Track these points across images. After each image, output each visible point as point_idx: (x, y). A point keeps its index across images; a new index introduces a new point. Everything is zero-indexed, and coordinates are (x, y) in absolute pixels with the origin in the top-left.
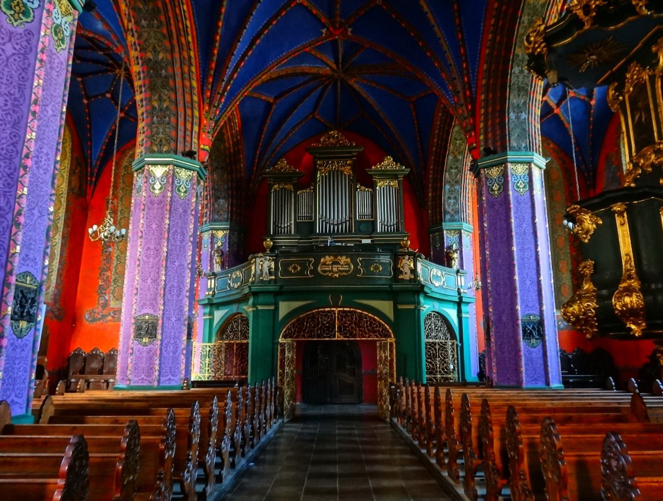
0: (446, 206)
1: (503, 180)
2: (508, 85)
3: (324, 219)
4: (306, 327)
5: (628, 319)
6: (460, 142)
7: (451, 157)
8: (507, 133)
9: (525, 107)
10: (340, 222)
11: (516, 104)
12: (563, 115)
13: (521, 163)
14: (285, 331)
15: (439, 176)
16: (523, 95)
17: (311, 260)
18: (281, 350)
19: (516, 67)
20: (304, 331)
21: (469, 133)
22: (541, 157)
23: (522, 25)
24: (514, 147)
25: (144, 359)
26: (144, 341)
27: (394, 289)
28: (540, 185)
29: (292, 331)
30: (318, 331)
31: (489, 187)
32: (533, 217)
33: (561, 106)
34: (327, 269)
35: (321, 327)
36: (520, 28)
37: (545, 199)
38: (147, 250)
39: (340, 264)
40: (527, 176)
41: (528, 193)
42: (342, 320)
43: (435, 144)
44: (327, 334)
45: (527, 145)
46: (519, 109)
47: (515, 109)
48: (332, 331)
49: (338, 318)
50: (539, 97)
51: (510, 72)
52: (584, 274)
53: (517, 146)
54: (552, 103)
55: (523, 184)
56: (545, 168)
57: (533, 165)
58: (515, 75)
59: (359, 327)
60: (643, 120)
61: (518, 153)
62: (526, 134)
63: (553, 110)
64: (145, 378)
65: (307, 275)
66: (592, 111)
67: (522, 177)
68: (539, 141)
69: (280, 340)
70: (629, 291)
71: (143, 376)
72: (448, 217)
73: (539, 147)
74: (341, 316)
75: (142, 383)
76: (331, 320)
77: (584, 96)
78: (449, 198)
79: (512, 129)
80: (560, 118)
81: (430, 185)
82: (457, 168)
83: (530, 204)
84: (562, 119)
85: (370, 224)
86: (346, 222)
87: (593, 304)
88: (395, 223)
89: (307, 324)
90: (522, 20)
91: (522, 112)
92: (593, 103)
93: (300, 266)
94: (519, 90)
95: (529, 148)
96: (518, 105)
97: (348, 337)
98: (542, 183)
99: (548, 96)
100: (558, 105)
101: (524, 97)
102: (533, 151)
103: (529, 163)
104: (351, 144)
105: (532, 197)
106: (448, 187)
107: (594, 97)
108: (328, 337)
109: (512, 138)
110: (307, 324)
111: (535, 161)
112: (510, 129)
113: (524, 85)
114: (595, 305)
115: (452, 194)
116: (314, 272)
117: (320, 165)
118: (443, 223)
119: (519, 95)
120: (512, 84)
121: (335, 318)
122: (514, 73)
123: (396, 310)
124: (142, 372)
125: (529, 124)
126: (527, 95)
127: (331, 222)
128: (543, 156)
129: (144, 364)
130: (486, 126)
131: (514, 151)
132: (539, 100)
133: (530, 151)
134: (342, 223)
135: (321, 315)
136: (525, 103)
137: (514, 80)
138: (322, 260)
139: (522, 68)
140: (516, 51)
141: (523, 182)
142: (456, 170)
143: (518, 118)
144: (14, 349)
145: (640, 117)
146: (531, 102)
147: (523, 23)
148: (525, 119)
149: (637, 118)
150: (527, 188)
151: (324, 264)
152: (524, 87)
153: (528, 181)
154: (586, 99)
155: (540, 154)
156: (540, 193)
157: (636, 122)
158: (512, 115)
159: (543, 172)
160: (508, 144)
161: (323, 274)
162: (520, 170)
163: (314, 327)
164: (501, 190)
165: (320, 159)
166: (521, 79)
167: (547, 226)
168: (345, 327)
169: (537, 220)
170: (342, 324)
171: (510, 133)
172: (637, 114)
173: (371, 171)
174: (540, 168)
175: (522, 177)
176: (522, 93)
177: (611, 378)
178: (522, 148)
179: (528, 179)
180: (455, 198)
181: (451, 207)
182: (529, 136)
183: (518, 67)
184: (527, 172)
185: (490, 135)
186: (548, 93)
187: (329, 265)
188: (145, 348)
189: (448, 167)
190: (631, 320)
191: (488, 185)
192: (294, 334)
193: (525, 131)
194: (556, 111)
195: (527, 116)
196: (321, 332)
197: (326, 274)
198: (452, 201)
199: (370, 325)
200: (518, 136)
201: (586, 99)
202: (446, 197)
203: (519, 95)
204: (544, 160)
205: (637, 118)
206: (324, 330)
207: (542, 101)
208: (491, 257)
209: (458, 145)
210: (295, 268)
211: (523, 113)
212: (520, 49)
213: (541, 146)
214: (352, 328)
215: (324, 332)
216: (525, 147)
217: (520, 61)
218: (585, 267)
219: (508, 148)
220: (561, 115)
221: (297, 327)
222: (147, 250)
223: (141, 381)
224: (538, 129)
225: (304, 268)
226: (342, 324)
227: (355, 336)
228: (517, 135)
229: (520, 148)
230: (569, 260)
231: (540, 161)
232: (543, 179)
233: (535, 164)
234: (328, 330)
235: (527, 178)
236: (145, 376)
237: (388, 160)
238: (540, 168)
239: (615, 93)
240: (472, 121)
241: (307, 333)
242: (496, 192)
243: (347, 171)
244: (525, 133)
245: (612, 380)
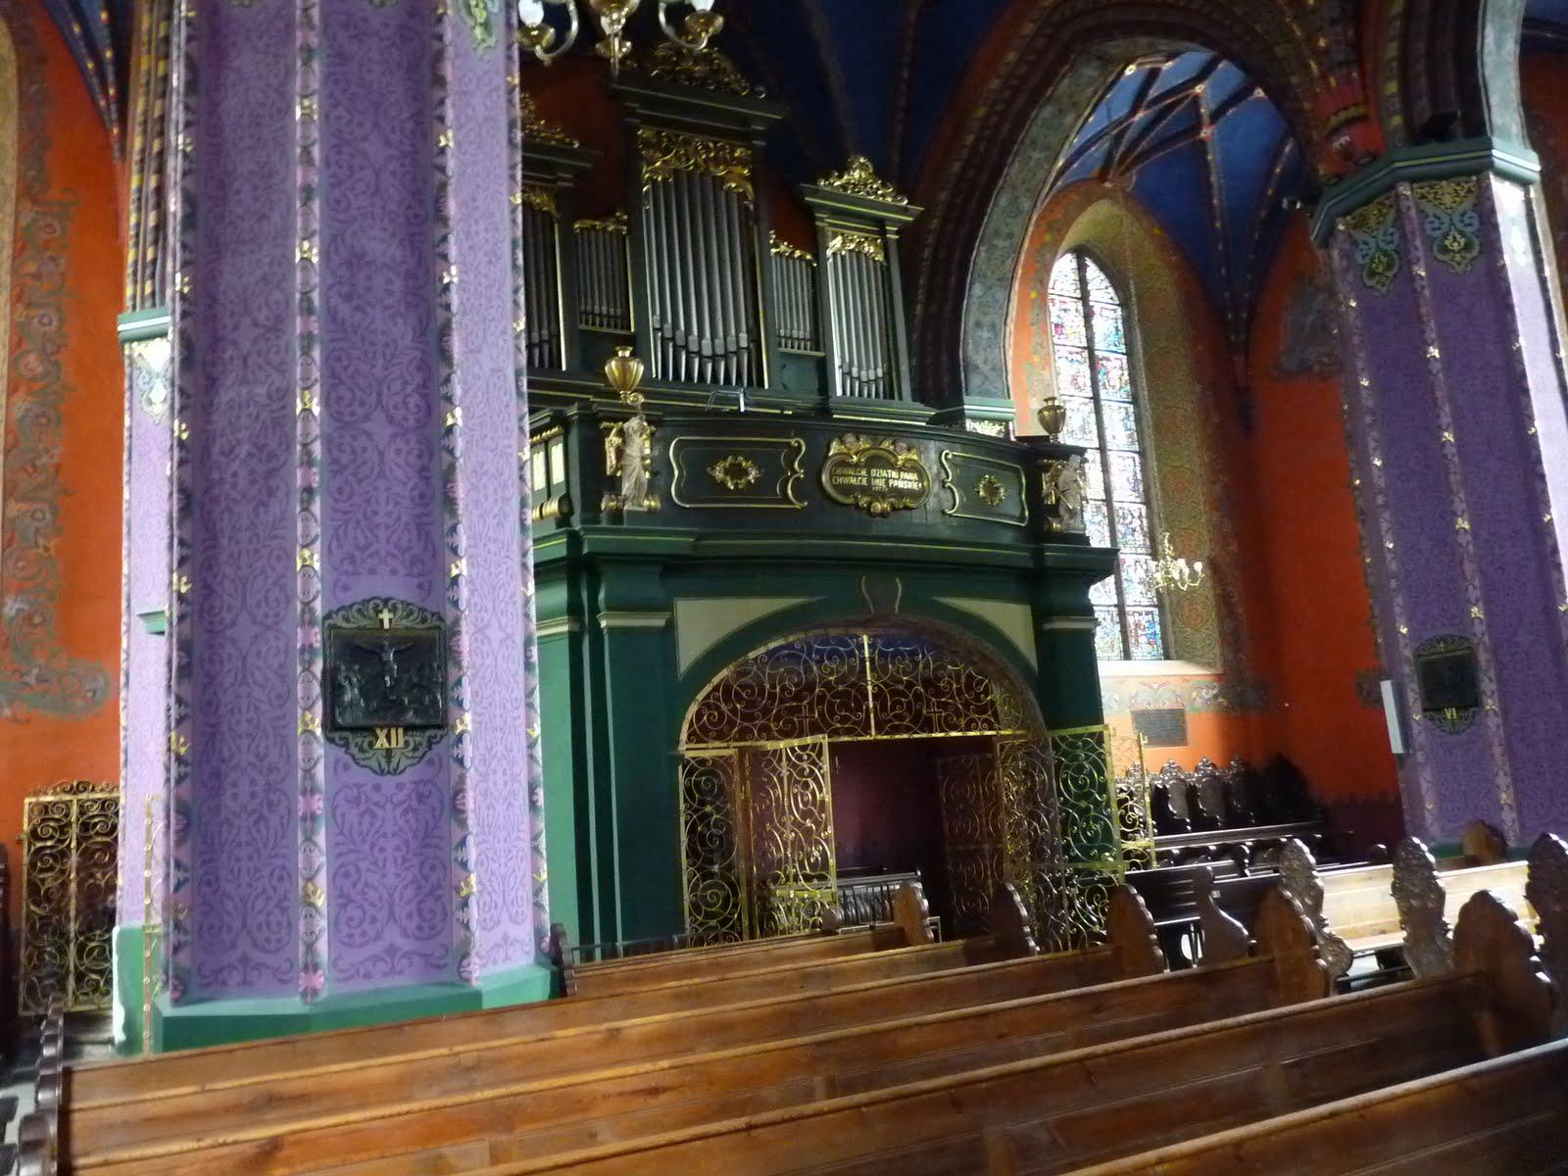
0: (970, 346)
1: (1476, 222)
3: (668, 334)
4: (772, 696)
6: (1042, 155)
7: (1003, 201)
10: (720, 351)
14: (699, 715)
15: (957, 256)
17: (793, 442)
18: (688, 790)
20: (766, 712)
21: (1344, 71)
25: (394, 842)
26: (382, 742)
27: (1049, 564)
29: (722, 714)
30: (811, 710)
31: (1433, 240)
34: (853, 481)
35: (821, 699)
38: (349, 264)
39: (893, 467)
42: (885, 670)
43: (965, 153)
44: (845, 719)
48: (859, 708)
49: (872, 660)
59: (939, 693)
64: (406, 945)
65: (786, 500)
69: (682, 747)
71: (393, 935)
72: (975, 381)
74: (882, 654)
75: (393, 972)
76: (851, 668)
78: (978, 325)
81: (922, 282)
82: (1010, 236)
85: (811, 366)
86: (737, 353)
88: (880, 374)
89: (773, 687)
93: (758, 465)
97: (908, 730)
100: (1216, 115)
104: (753, 93)
106: (978, 290)
108: (848, 732)
110: (773, 687)
115: (984, 314)
116: (810, 486)
117: (647, 144)
118: (966, 399)
121: (863, 660)
123: (1044, 639)
124: (382, 916)
127: (694, 347)
129: (391, 869)
130: (1404, 60)
134: (726, 356)
135: (818, 652)
138: (835, 448)
142: (1007, 244)
144: (261, 758)
151: (843, 463)
161: (840, 498)
163: (798, 697)
164: (1475, 253)
165: (648, 121)
168: (894, 693)
170: (884, 684)
173: (816, 193)
180: (993, 327)
181: (982, 353)
185: (1423, 83)
187: (857, 466)
188: (389, 782)
189: (992, 226)
191: (1429, 232)
192: (732, 724)
196: (821, 714)
197: (850, 500)
198: (985, 334)
199: (969, 687)
202: (972, 321)
206: (831, 705)
208: (1460, 453)
209: (1032, 164)
210: (737, 472)
214: (918, 697)
215: (832, 713)
221: (739, 698)
222: (349, 264)
223: (382, 966)
225: (773, 473)
226: (884, 684)
227: (928, 726)
230: (1205, 533)
234: (845, 706)
236: (405, 933)
237: (862, 167)
240: (1350, 33)
241: (778, 718)
242: (1458, 257)
243: (737, 180)
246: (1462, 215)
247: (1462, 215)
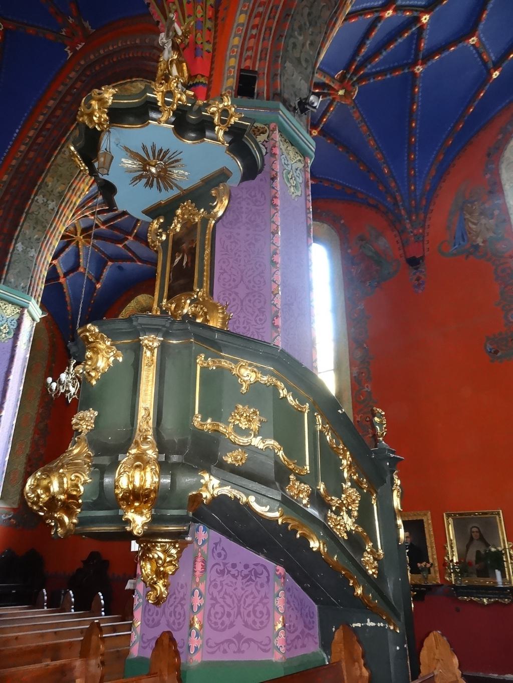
2: (26, 210)
5: (130, 506)
8: (7, 263)
9: (39, 244)
11: (27, 237)
12: (67, 287)
13: (13, 303)
16: (38, 231)
19: (41, 196)
22: (38, 307)
23: (61, 154)
24: (11, 282)
28: (27, 339)
32: (8, 372)
33: (68, 277)
36: (59, 157)
37: (28, 356)
40: (15, 321)
41: (11, 341)
45: (26, 287)
46: (30, 243)
47: (25, 241)
50: (50, 259)
51: (32, 197)
52: (77, 430)
53: (15, 282)
54: (60, 271)
55: (8, 330)
56: (38, 321)
57: (26, 311)
58: (38, 204)
60: (184, 264)
61: (15, 291)
62: (29, 274)
63: (58, 277)
66: (95, 294)
67: (9, 320)
68: (41, 289)
70: (141, 462)
73: (39, 295)
77: (93, 276)
79: (15, 261)
80: (63, 288)
83: (8, 356)
84: (65, 291)
87: (85, 478)
90: (63, 150)
91: (32, 249)
92: (98, 286)
94: (36, 223)
95: (28, 290)
96: (30, 238)
98: (30, 337)
99: (58, 262)
100: (66, 275)
101: (41, 233)
102: (31, 296)
103: (23, 308)
105: (14, 347)
107: (101, 281)
109: (11, 272)
111: (30, 308)
112: (12, 260)
113: (44, 220)
114: (87, 478)
119: (34, 228)
120: (30, 211)
122: (37, 201)
125: (36, 264)
126: (43, 232)
128: (41, 307)
131: (9, 286)
132: (54, 247)
133: (28, 294)
136: (38, 239)
137: (34, 208)
139: (48, 200)
140: (47, 179)
141: (9, 327)
143: (25, 251)
145: (182, 260)
146: (46, 242)
147: (64, 153)
148: (33, 257)
149: (177, 260)
150: (11, 336)
152: (43, 222)
153: (15, 327)
154: (94, 280)
155: (37, 303)
156: (25, 347)
157: (175, 264)
158: (20, 246)
159: (35, 325)
160: (4, 277)
162: (9, 312)
166: (42, 211)
167: (21, 388)
169: (11, 377)
171: (11, 265)
172: (179, 256)
174: (33, 320)
175: (9, 320)
176: (39, 227)
177: (44, 591)
178: (20, 288)
179: (16, 325)
182: (32, 277)
183: (43, 197)
184: (17, 317)
186: (60, 258)
190: (135, 508)
193: (30, 271)
194: (62, 280)
195: (36, 255)
200: (19, 272)
201: (94, 280)
203: (34, 228)
204: (40, 312)
205: (177, 260)
207: (51, 264)
211: (33, 250)
212: (51, 179)
213: (41, 295)
216: (23, 288)
217: (48, 191)
218: (83, 419)
219: (3, 280)
220: (65, 286)
224: (44, 276)
228: (18, 270)
229: (16, 287)
231: (35, 311)
232: (33, 333)
233: (28, 311)
235: (15, 323)
238: (33, 320)
239: (159, 228)
244: (29, 271)
245: (45, 593)
246: (12, 320)
247: (12, 320)
